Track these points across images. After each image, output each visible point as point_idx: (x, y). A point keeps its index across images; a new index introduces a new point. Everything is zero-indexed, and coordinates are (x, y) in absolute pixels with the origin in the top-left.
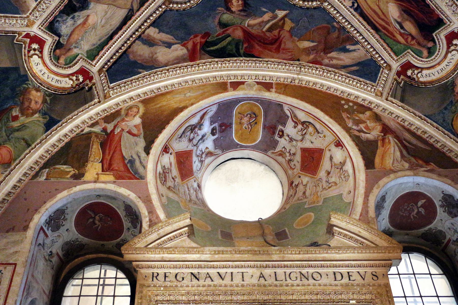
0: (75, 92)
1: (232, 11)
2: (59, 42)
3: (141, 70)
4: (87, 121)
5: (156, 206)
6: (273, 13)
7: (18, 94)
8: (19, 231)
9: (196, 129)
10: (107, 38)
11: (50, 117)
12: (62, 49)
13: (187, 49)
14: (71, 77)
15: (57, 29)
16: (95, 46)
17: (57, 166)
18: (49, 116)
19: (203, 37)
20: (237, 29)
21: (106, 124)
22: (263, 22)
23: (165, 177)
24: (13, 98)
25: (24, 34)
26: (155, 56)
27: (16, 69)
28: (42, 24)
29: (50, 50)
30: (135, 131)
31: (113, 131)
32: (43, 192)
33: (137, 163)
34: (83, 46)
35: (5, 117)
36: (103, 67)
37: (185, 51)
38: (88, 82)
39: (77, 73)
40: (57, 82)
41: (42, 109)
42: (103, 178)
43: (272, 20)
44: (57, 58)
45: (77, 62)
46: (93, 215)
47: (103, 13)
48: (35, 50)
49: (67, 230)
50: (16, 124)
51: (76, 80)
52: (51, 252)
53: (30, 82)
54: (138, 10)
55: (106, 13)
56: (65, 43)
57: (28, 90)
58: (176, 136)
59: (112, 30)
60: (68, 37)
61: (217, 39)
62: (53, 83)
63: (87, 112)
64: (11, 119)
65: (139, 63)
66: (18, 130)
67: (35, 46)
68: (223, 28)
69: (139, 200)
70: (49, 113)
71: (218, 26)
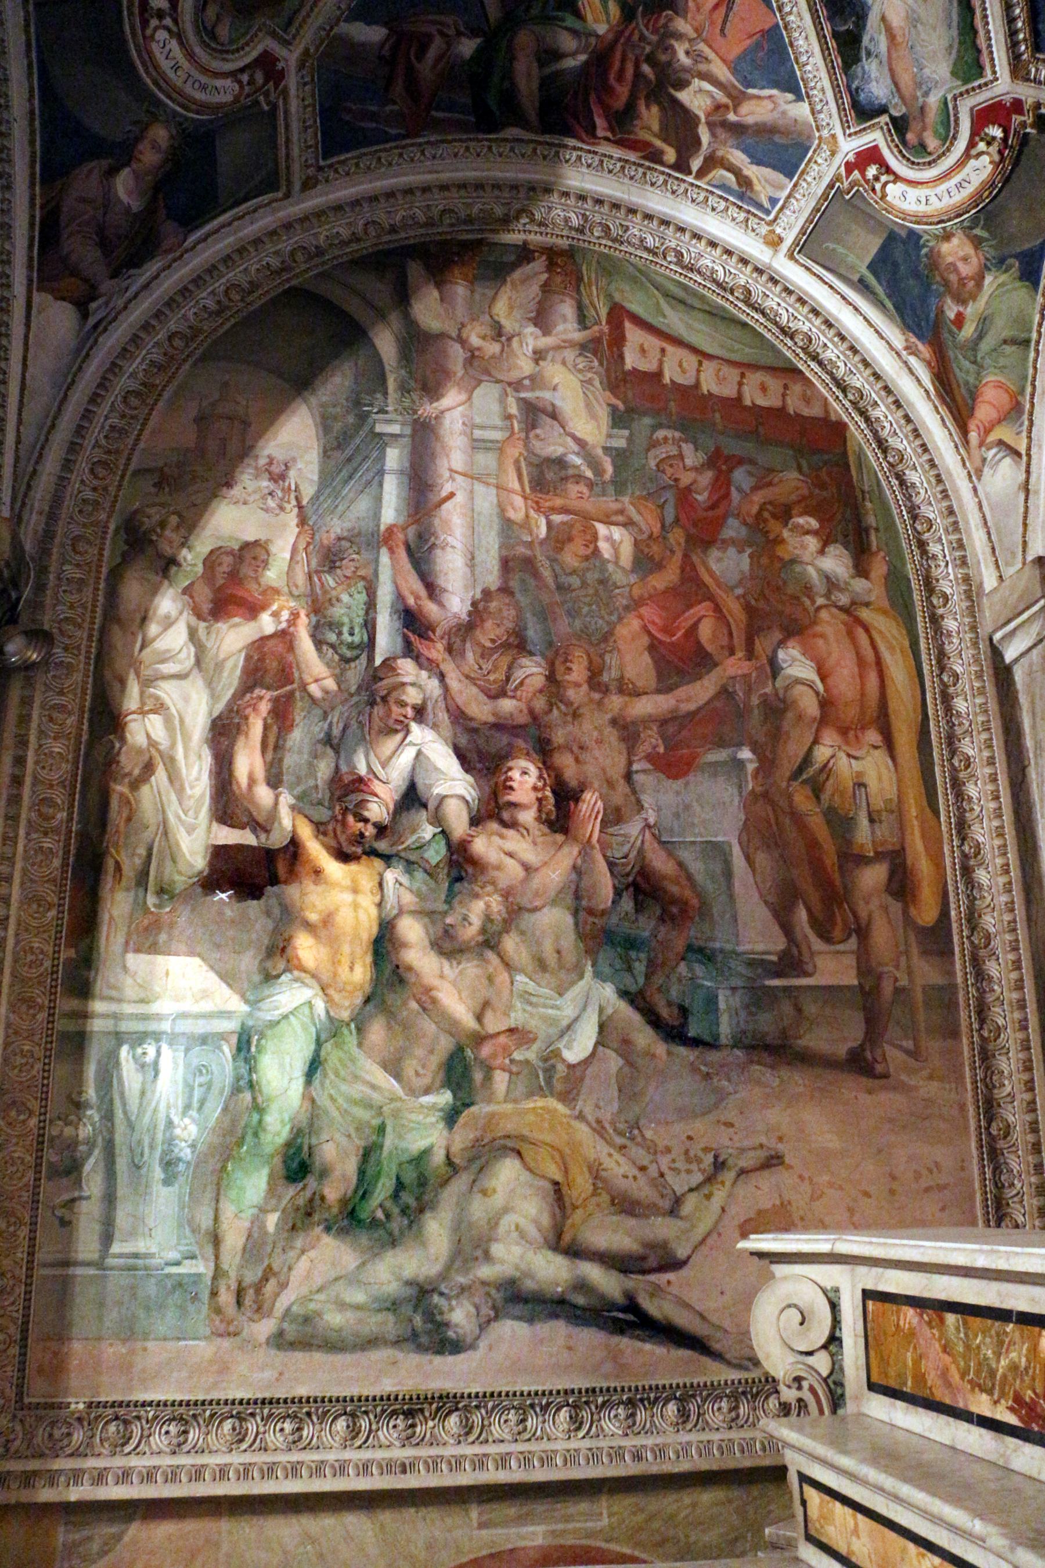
0: (1016, 163)
2: (893, 119)
11: (1016, 256)
14: (974, 152)
15: (871, 103)
18: (1011, 256)
24: (927, 287)
27: (892, 238)
28: (845, 125)
29: (895, 150)
35: (946, 335)
39: (976, 132)
41: (987, 259)
48: (877, 179)
50: (968, 331)
51: (989, 144)
53: (926, 237)
56: (904, 110)
64: (955, 330)
67: (872, 171)
70: (1006, 251)
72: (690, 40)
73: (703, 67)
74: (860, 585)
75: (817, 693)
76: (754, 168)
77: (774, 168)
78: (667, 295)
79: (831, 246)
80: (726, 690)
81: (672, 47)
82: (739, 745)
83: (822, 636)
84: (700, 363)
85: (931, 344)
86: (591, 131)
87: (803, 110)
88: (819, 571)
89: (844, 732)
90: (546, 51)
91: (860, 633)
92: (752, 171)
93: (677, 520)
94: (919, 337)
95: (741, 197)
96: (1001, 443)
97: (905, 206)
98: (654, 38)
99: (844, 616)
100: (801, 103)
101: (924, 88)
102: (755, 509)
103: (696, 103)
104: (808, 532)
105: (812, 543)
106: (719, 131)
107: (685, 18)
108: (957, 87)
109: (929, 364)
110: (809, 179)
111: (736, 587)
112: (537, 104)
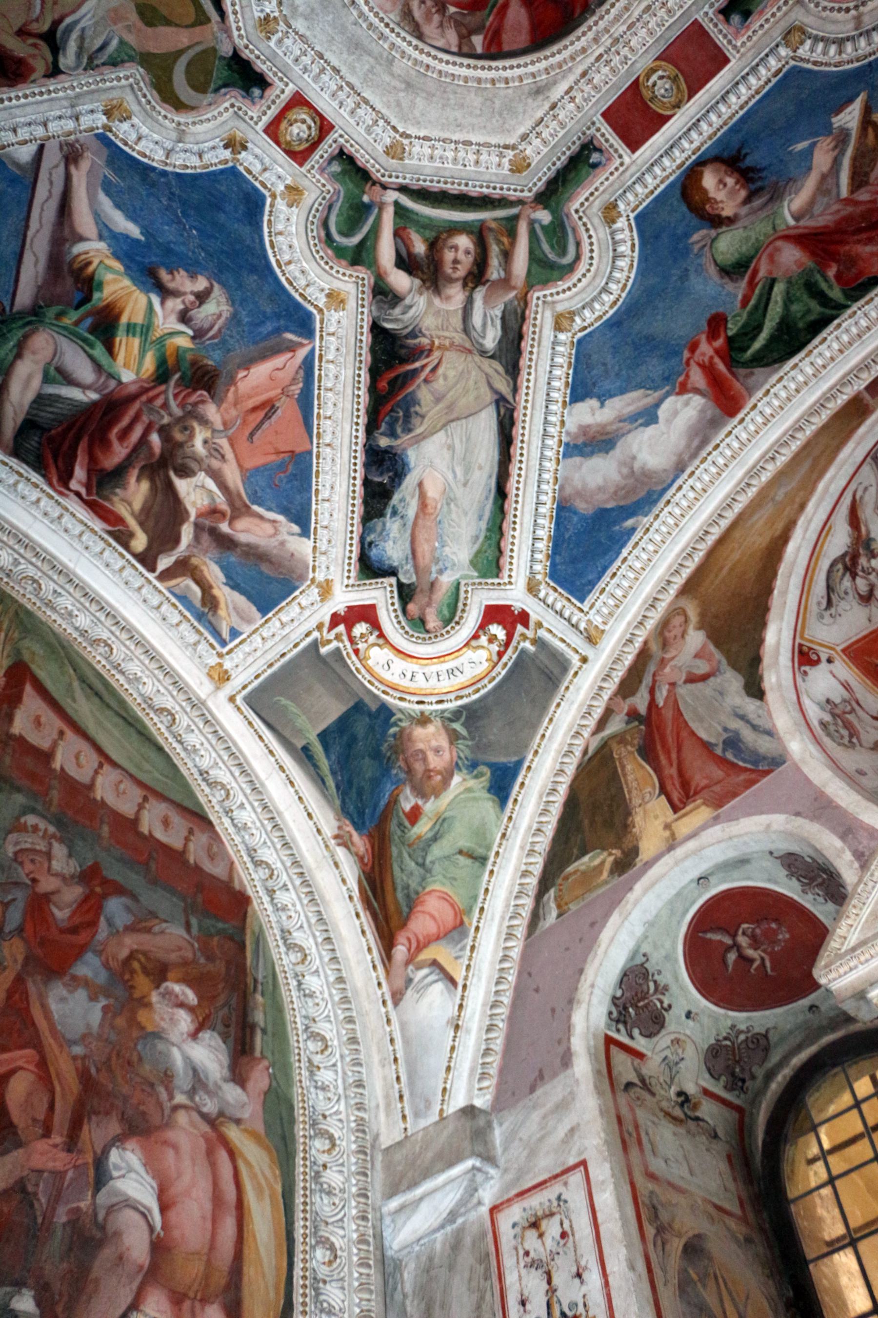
1: (728, 218)
3: (629, 523)
5: (851, 809)
6: (830, 133)
8: (555, 1075)
9: (863, 561)
10: (495, 502)
11: (490, 765)
13: (697, 391)
14: (474, 643)
15: (380, 561)
16: (481, 539)
17: (570, 869)
19: (712, 335)
20: (778, 250)
21: (630, 701)
22: (824, 177)
23: (848, 725)
24: (386, 772)
26: (637, 466)
27: (359, 707)
29: (393, 615)
30: (702, 667)
31: (652, 704)
32: (567, 949)
33: (748, 735)
35: (393, 826)
37: (697, 401)
38: (520, 628)
39: (482, 627)
42: (684, 826)
43: (842, 153)
44: (420, 623)
46: (728, 941)
47: (447, 454)
49: (688, 1015)
52: (680, 1094)
53: (399, 715)
54: (515, 390)
55: (451, 448)
56: (414, 579)
57: (405, 737)
58: (813, 608)
59: (490, 477)
60: (411, 561)
61: (751, 314)
62: (446, 685)
64: (407, 824)
65: (612, 509)
66: (435, 839)
67: (360, 629)
68: (742, 276)
69: (800, 821)
70: (481, 757)
71: (726, 280)
72: (214, 431)
73: (215, 464)
74: (232, 1093)
75: (151, 1228)
76: (227, 590)
77: (250, 598)
78: (83, 680)
79: (284, 701)
80: (23, 1190)
81: (192, 430)
82: (19, 1284)
83: (175, 1148)
84: (101, 766)
85: (370, 836)
86: (65, 477)
87: (303, 547)
88: (187, 1059)
89: (177, 1299)
90: (59, 370)
91: (223, 1156)
92: (223, 593)
93: (20, 930)
94: (358, 827)
95: (200, 617)
96: (435, 963)
97: (386, 676)
98: (178, 412)
99: (206, 1128)
100: (305, 540)
101: (441, 565)
102: (124, 953)
103: (192, 497)
104: (182, 1005)
105: (185, 1021)
106: (206, 538)
107: (219, 406)
108: (472, 577)
109: (361, 859)
111: (75, 1043)
112: (20, 419)
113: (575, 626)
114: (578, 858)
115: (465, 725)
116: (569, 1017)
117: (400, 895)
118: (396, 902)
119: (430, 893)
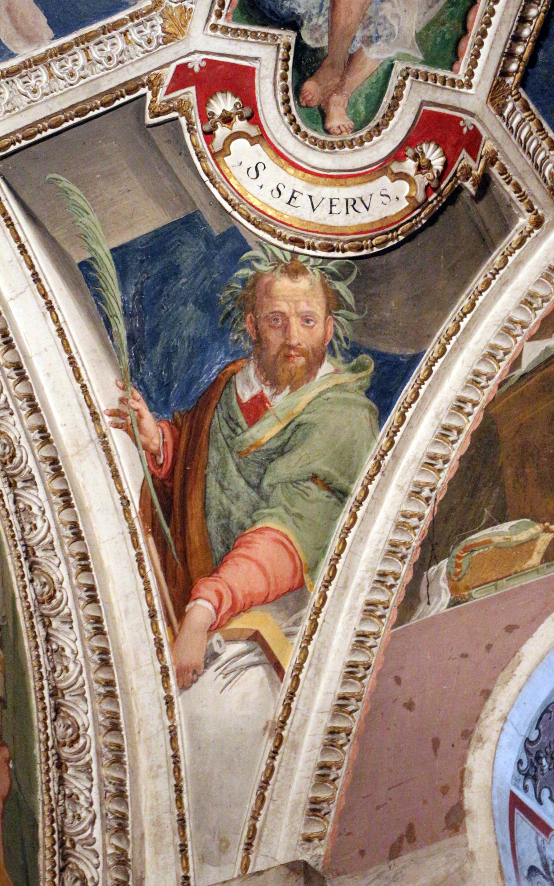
0: (433, 220)
2: (300, 45)
4: (519, 316)
7: (229, 314)
8: (434, 839)
11: (377, 355)
12: (321, 73)
14: (395, 167)
17: (478, 537)
18: (369, 352)
25: (168, 74)
29: (280, 95)
32: (464, 656)
34: (394, 22)
36: (505, 74)
40: (351, 210)
45: (396, 99)
48: (227, 119)
51: (419, 168)
53: (257, 252)
56: (325, 43)
57: (261, 286)
63: (505, 283)
64: (241, 419)
70: (367, 341)
79: (65, 183)
85: (175, 426)
109: (153, 456)
110: (94, 53)
113: (539, 168)
114: (490, 524)
115: (353, 288)
116: (464, 759)
117: (213, 525)
118: (205, 534)
119: (260, 531)
